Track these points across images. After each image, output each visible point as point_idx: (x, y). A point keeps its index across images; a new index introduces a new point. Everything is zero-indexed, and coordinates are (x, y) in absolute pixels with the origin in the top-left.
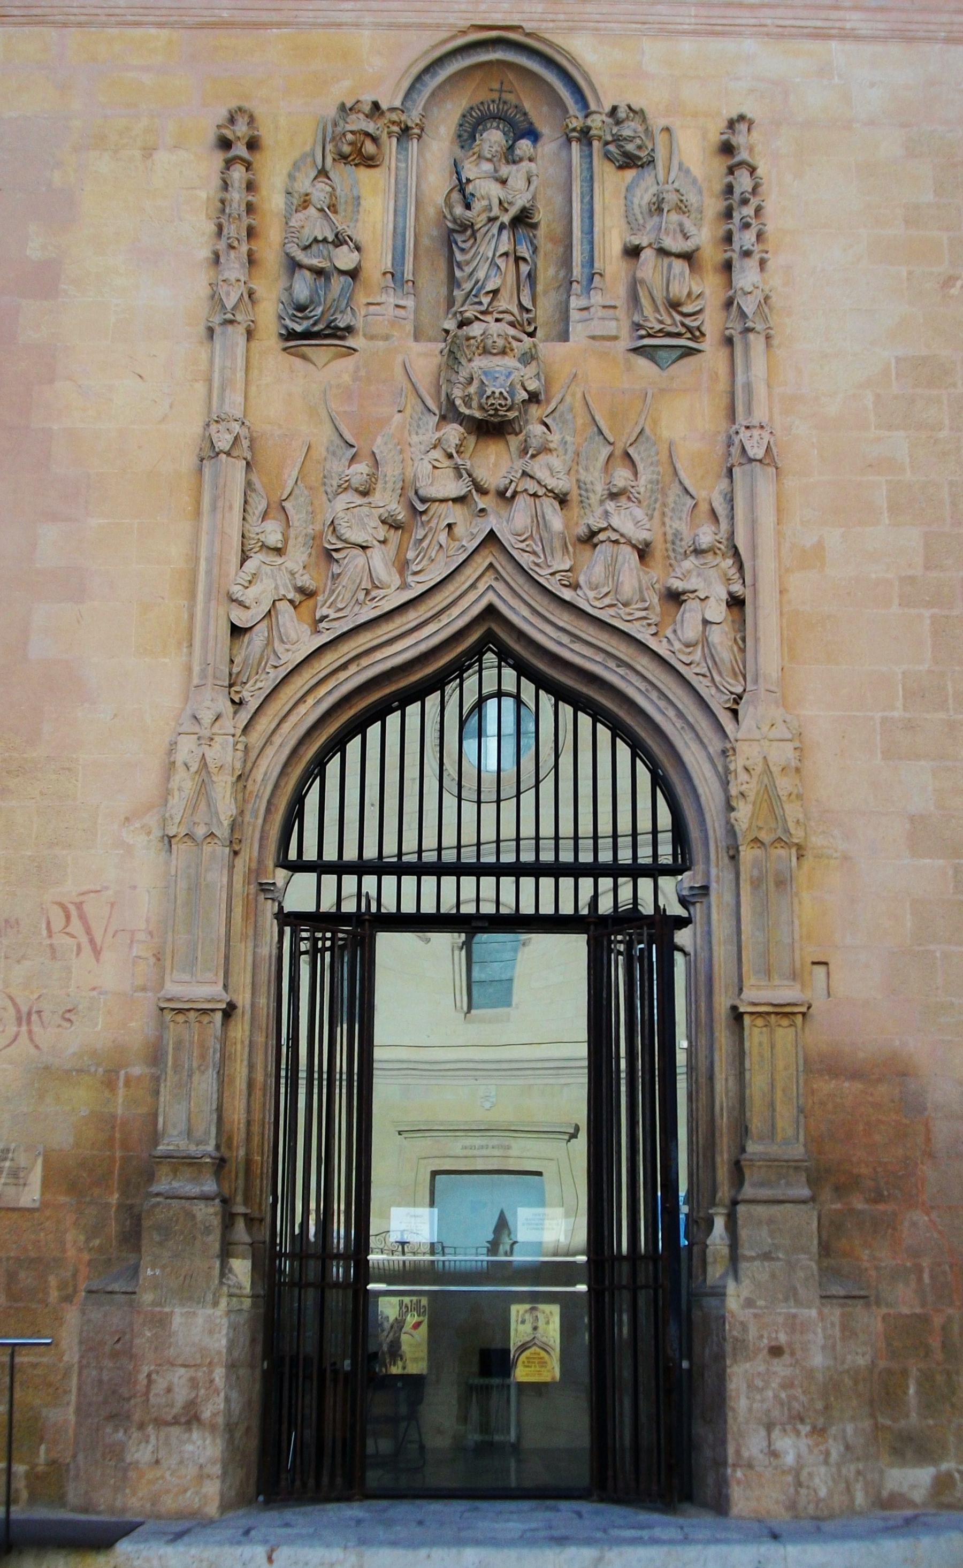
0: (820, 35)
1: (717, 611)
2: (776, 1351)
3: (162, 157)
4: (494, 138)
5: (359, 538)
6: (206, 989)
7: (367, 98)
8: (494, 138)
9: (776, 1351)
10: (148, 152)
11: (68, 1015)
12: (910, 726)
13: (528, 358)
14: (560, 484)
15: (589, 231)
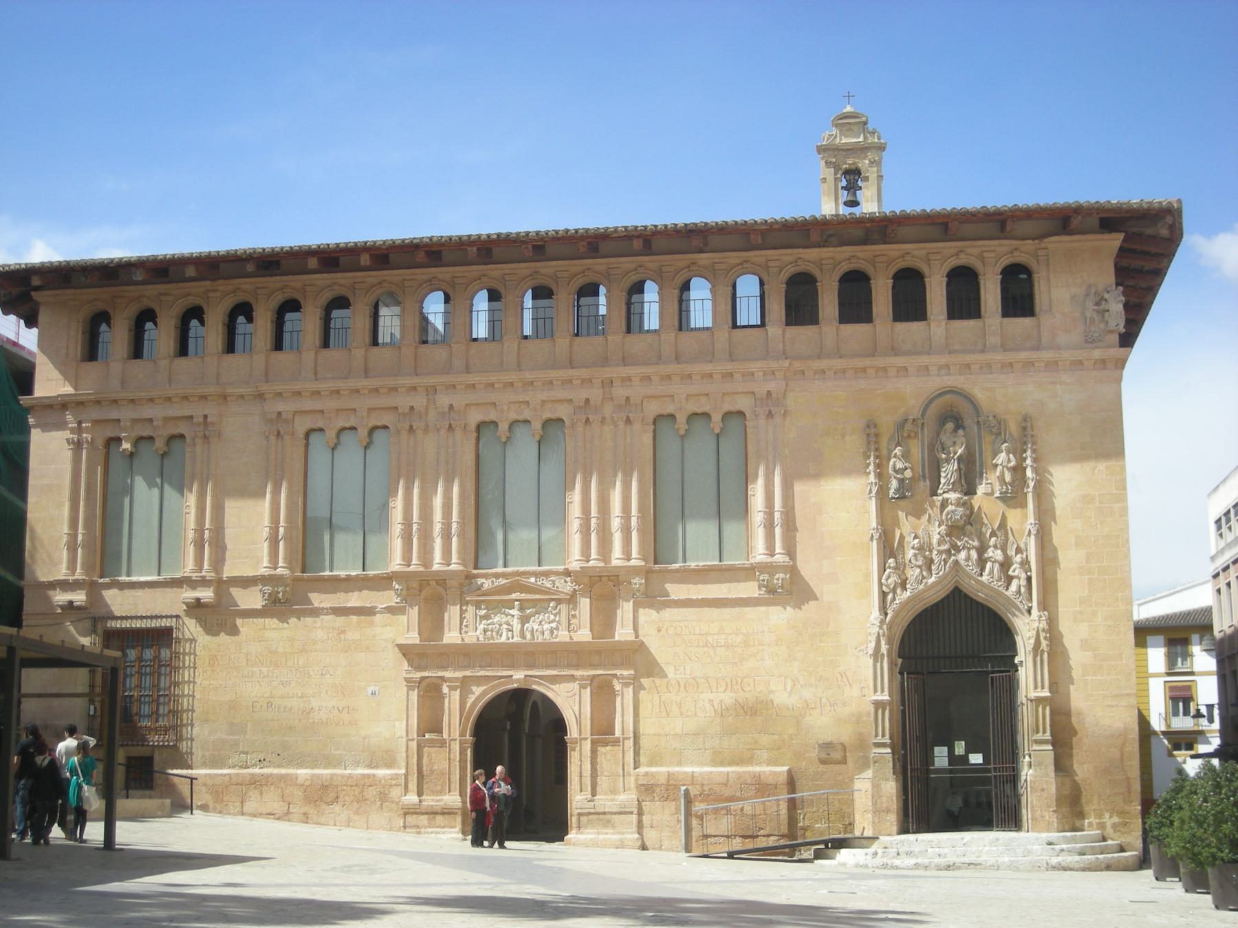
0: (1054, 383)
1: (1023, 582)
2: (1043, 790)
3: (848, 438)
4: (950, 426)
5: (920, 563)
6: (886, 697)
7: (911, 417)
8: (950, 426)
9: (1043, 790)
10: (843, 436)
11: (844, 704)
12: (1081, 612)
13: (964, 504)
14: (976, 543)
15: (981, 454)
